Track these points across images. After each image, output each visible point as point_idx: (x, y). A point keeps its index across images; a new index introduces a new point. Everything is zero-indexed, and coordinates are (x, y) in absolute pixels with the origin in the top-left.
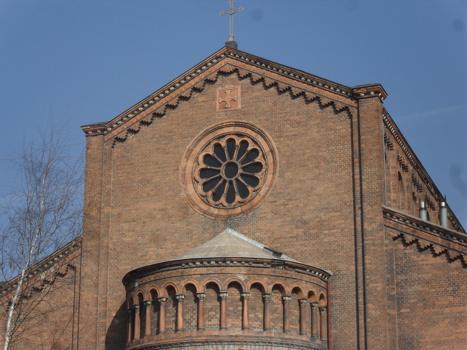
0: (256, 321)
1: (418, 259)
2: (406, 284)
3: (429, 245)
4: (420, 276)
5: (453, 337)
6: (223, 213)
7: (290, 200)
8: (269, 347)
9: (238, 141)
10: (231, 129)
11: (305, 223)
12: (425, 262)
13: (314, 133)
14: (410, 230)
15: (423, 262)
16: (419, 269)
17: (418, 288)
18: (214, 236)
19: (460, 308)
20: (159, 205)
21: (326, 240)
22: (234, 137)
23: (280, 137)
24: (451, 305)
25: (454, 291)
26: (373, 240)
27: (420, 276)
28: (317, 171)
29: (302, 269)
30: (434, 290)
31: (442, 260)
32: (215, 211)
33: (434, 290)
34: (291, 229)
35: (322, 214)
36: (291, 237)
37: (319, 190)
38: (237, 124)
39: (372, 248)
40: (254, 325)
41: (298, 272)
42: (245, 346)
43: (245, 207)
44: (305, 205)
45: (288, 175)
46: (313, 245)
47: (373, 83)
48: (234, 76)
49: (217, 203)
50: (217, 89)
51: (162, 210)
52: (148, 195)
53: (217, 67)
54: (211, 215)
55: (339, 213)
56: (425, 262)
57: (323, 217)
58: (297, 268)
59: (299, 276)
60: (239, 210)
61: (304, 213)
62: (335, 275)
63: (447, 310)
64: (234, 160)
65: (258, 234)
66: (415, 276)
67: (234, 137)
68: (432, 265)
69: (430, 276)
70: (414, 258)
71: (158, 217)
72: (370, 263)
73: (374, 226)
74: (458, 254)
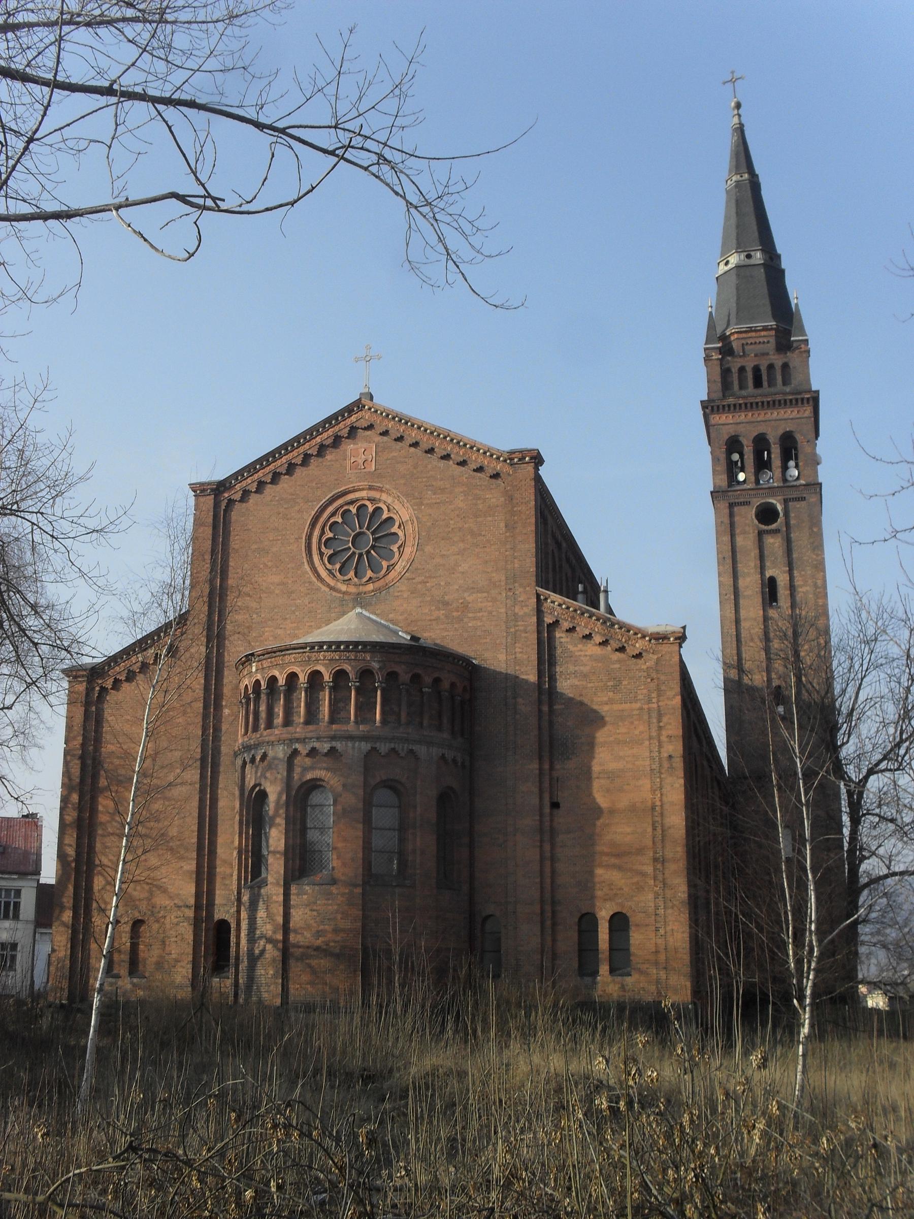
1: (575, 649)
4: (576, 668)
5: (611, 739)
6: (352, 589)
7: (430, 577)
9: (371, 509)
10: (364, 494)
11: (446, 604)
12: (583, 653)
13: (460, 502)
15: (580, 653)
18: (343, 615)
20: (276, 579)
21: (470, 625)
22: (367, 503)
23: (422, 504)
25: (615, 686)
27: (576, 668)
28: (461, 545)
30: (592, 685)
32: (343, 588)
33: (592, 685)
34: (430, 610)
35: (466, 595)
36: (431, 620)
37: (464, 567)
38: (371, 488)
39: (523, 635)
43: (378, 584)
45: (428, 549)
46: (456, 630)
47: (530, 447)
49: (346, 578)
50: (349, 447)
51: (283, 584)
52: (266, 566)
53: (348, 422)
54: (339, 591)
55: (485, 594)
56: (583, 653)
57: (470, 599)
60: (371, 587)
64: (364, 530)
65: (391, 616)
66: (572, 668)
67: (367, 503)
68: (591, 656)
69: (588, 668)
71: (277, 592)
73: (526, 610)
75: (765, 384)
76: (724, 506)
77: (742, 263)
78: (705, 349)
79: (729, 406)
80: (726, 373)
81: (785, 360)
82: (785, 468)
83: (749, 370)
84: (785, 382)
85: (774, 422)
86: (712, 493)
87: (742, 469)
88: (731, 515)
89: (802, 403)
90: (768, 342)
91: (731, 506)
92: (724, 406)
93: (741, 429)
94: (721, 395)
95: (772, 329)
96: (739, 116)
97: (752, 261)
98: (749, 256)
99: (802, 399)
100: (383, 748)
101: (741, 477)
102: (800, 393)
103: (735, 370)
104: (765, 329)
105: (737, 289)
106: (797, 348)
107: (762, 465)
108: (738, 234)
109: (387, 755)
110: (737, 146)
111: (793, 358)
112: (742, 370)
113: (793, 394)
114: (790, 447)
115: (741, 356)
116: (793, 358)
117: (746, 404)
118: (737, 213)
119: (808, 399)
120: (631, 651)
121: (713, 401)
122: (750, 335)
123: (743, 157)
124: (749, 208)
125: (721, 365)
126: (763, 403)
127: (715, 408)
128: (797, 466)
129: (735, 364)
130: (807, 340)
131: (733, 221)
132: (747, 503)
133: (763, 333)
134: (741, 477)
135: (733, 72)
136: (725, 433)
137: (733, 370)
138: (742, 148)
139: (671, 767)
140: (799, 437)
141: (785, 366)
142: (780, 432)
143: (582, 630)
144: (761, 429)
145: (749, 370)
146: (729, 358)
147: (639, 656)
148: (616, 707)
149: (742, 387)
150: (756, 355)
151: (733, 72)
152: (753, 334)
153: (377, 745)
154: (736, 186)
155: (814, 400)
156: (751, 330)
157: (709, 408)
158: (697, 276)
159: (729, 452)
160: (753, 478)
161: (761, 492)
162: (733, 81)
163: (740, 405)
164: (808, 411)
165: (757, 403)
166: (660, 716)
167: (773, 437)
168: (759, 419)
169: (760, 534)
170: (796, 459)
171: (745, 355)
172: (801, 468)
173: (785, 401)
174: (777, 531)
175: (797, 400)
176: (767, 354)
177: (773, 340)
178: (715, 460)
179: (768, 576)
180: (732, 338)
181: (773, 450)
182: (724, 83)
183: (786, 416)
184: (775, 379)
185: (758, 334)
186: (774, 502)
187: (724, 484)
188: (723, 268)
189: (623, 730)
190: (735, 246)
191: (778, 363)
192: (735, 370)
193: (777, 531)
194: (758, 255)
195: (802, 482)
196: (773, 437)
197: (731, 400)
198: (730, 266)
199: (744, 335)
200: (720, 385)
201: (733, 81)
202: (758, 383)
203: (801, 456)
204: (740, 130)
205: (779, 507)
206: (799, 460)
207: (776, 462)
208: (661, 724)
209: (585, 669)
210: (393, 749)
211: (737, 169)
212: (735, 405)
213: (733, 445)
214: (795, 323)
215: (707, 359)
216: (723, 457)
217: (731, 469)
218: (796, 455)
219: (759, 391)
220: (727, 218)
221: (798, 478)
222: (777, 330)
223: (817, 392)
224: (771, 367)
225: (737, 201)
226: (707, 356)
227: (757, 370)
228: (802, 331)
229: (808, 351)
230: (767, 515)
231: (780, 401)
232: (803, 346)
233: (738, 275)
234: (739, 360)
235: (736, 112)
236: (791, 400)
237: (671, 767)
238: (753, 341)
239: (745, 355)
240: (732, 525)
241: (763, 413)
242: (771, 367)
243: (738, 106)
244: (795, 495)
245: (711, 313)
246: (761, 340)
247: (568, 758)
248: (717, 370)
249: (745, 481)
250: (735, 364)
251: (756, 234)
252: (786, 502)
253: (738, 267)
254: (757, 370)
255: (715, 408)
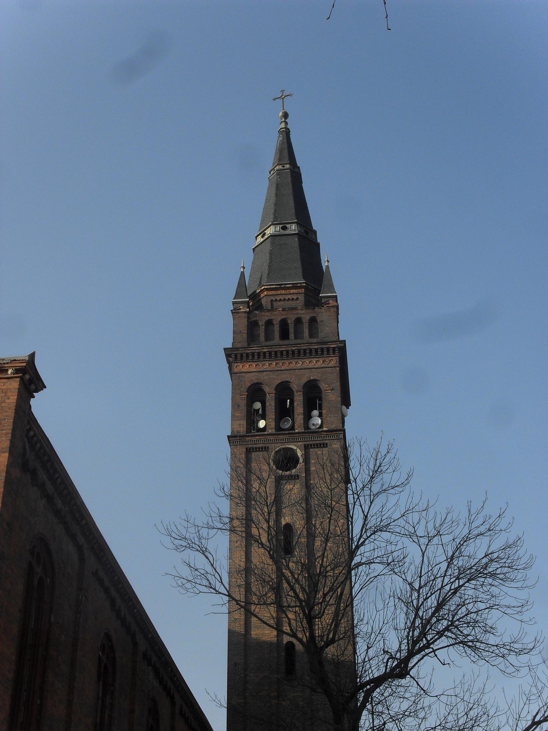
75: (292, 336)
76: (241, 451)
77: (277, 233)
78: (234, 303)
79: (253, 354)
80: (252, 326)
81: (312, 315)
82: (308, 417)
83: (276, 322)
84: (311, 336)
85: (299, 372)
86: (229, 437)
87: (263, 417)
88: (248, 461)
89: (328, 353)
90: (297, 299)
91: (249, 451)
92: (247, 355)
93: (264, 377)
94: (245, 345)
95: (301, 287)
96: (286, 123)
97: (287, 232)
98: (284, 228)
99: (328, 349)
101: (262, 424)
102: (326, 343)
103: (262, 323)
104: (295, 287)
105: (271, 254)
106: (325, 303)
107: (284, 412)
108: (275, 211)
110: (282, 144)
111: (323, 315)
112: (269, 323)
113: (318, 343)
114: (313, 397)
115: (269, 311)
116: (323, 315)
117: (270, 353)
118: (276, 195)
119: (334, 349)
121: (237, 349)
122: (279, 292)
123: (287, 152)
124: (288, 190)
125: (249, 318)
126: (287, 352)
127: (239, 356)
128: (320, 415)
129: (262, 318)
130: (336, 297)
131: (273, 199)
132: (266, 449)
133: (292, 291)
134: (262, 424)
135: (283, 91)
136: (248, 380)
137: (260, 323)
138: (286, 146)
140: (323, 386)
141: (313, 321)
142: (305, 380)
144: (285, 377)
145: (276, 322)
146: (256, 312)
149: (267, 339)
150: (284, 310)
151: (283, 91)
152: (283, 292)
154: (278, 174)
155: (341, 351)
156: (280, 287)
157: (233, 356)
158: (233, 243)
159: (250, 401)
160: (273, 424)
161: (281, 437)
162: (282, 98)
163: (265, 353)
164: (334, 361)
165: (282, 352)
167: (297, 385)
168: (283, 368)
169: (279, 480)
170: (320, 409)
171: (272, 309)
172: (324, 416)
173: (311, 350)
174: (297, 477)
175: (322, 349)
176: (295, 309)
177: (302, 298)
178: (235, 406)
179: (283, 523)
180: (262, 295)
181: (295, 398)
182: (275, 99)
183: (310, 366)
184: (303, 332)
185: (287, 292)
186: (295, 448)
187: (243, 430)
188: (260, 240)
190: (272, 220)
191: (306, 316)
192: (262, 323)
193: (297, 477)
194: (294, 227)
195: (325, 429)
196: (297, 385)
197: (255, 349)
198: (266, 237)
199: (274, 292)
200: (245, 336)
201: (282, 98)
202: (285, 335)
203: (325, 404)
204: (286, 133)
205: (299, 453)
206: (323, 408)
207: (299, 409)
211: (280, 161)
212: (259, 354)
213: (255, 392)
214: (325, 282)
215: (235, 312)
216: (243, 403)
217: (252, 418)
218: (320, 405)
219: (286, 342)
220: (267, 200)
221: (321, 426)
222: (306, 288)
223: (345, 341)
224: (298, 321)
225: (277, 185)
226: (235, 309)
227: (284, 324)
228: (331, 288)
229: (337, 307)
230: (287, 460)
231: (305, 350)
232: (331, 301)
233: (272, 243)
234: (267, 314)
235: (283, 120)
236: (316, 350)
238: (282, 297)
239: (272, 309)
240: (249, 470)
241: (287, 362)
242: (298, 321)
243: (286, 115)
244: (316, 440)
245: (243, 274)
246: (290, 297)
248: (245, 322)
249: (264, 429)
250: (262, 318)
251: (293, 210)
252: (306, 448)
253: (272, 236)
254: (284, 324)
255: (239, 356)
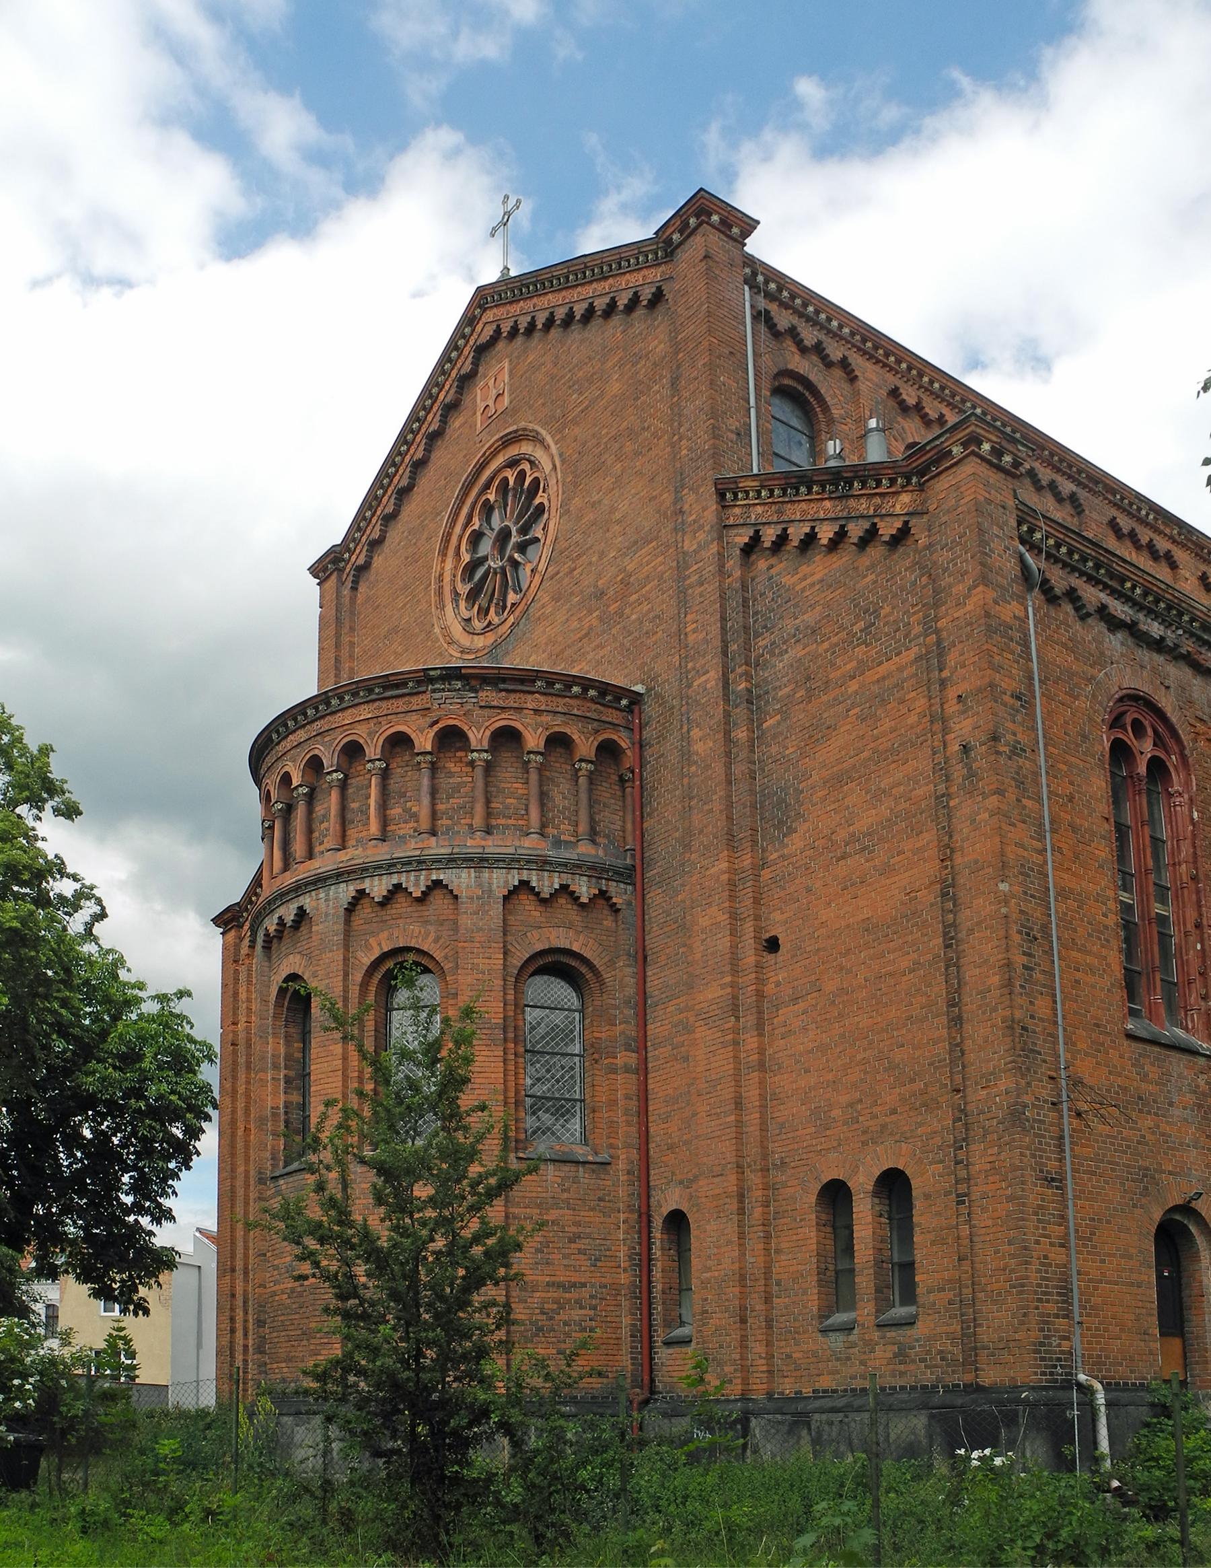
0: (406, 822)
2: (772, 654)
3: (807, 530)
8: (424, 872)
14: (770, 514)
16: (796, 606)
17: (796, 652)
19: (879, 669)
24: (863, 667)
26: (699, 571)
29: (522, 681)
30: (826, 645)
31: (840, 560)
33: (826, 645)
40: (401, 832)
41: (507, 691)
42: (367, 881)
44: (602, 555)
48: (501, 345)
57: (630, 568)
58: (504, 680)
59: (512, 700)
61: (599, 576)
62: (649, 690)
63: (853, 686)
66: (789, 625)
68: (822, 581)
70: (787, 580)
72: (695, 631)
73: (701, 536)
74: (867, 525)
100: (378, 887)
109: (386, 901)
120: (887, 529)
139: (971, 774)
143: (797, 533)
147: (902, 536)
148: (871, 676)
153: (366, 885)
166: (941, 654)
189: (887, 724)
208: (946, 674)
209: (810, 618)
210: (398, 887)
237: (971, 774)
247: (792, 830)
